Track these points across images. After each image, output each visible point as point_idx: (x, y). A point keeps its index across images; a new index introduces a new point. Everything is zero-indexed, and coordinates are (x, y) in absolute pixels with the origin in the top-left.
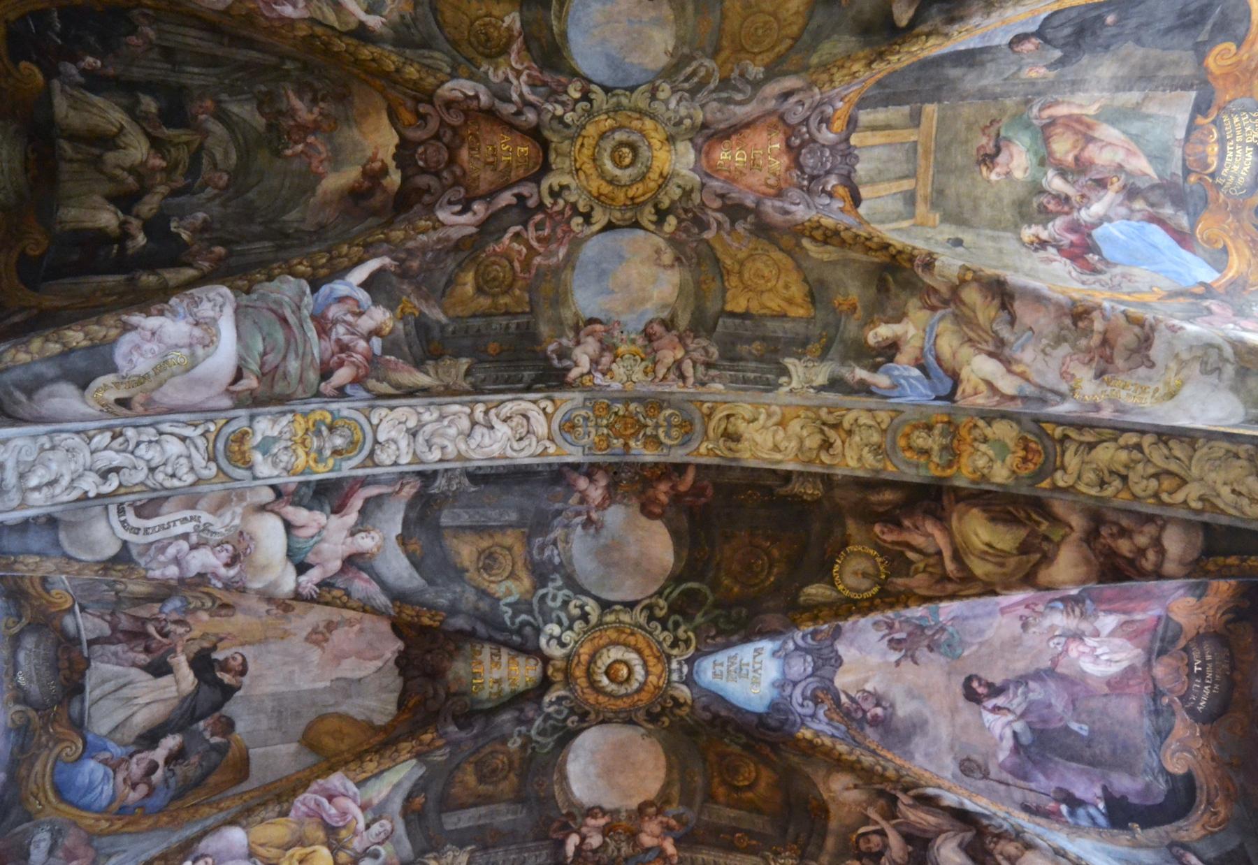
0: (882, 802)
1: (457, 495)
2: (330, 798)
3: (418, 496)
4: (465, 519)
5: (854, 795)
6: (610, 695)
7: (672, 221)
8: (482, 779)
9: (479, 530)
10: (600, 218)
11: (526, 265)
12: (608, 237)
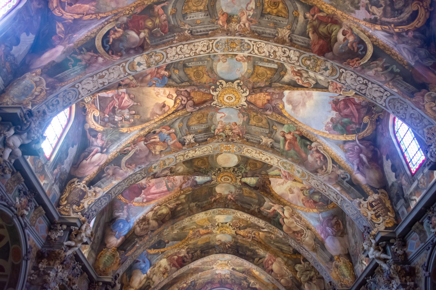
0: (173, 171)
1: (254, 204)
2: (286, 176)
3: (261, 207)
4: (254, 200)
5: (178, 169)
6: (228, 176)
7: (216, 224)
8: (256, 164)
9: (251, 197)
10: (228, 225)
11: (240, 221)
12: (226, 222)
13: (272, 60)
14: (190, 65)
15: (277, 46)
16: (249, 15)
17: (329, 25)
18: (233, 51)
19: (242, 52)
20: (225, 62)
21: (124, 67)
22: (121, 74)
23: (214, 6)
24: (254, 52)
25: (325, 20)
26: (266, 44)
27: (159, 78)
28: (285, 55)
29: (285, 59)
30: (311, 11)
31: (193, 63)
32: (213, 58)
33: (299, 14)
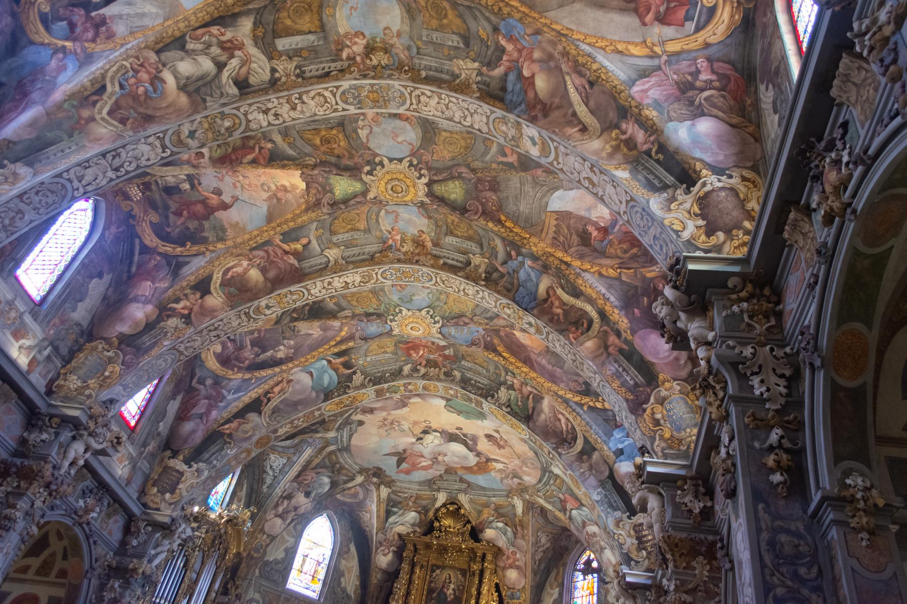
13: (292, 92)
14: (454, 40)
15: (294, 119)
16: (363, 120)
17: (230, 150)
18: (372, 85)
19: (354, 85)
20: (386, 28)
21: (556, 158)
22: (563, 153)
23: (425, 132)
24: (331, 92)
25: (240, 152)
26: (315, 115)
27: (517, 40)
28: (273, 111)
29: (270, 105)
30: (267, 152)
31: (450, 43)
32: (413, 44)
33: (284, 140)
